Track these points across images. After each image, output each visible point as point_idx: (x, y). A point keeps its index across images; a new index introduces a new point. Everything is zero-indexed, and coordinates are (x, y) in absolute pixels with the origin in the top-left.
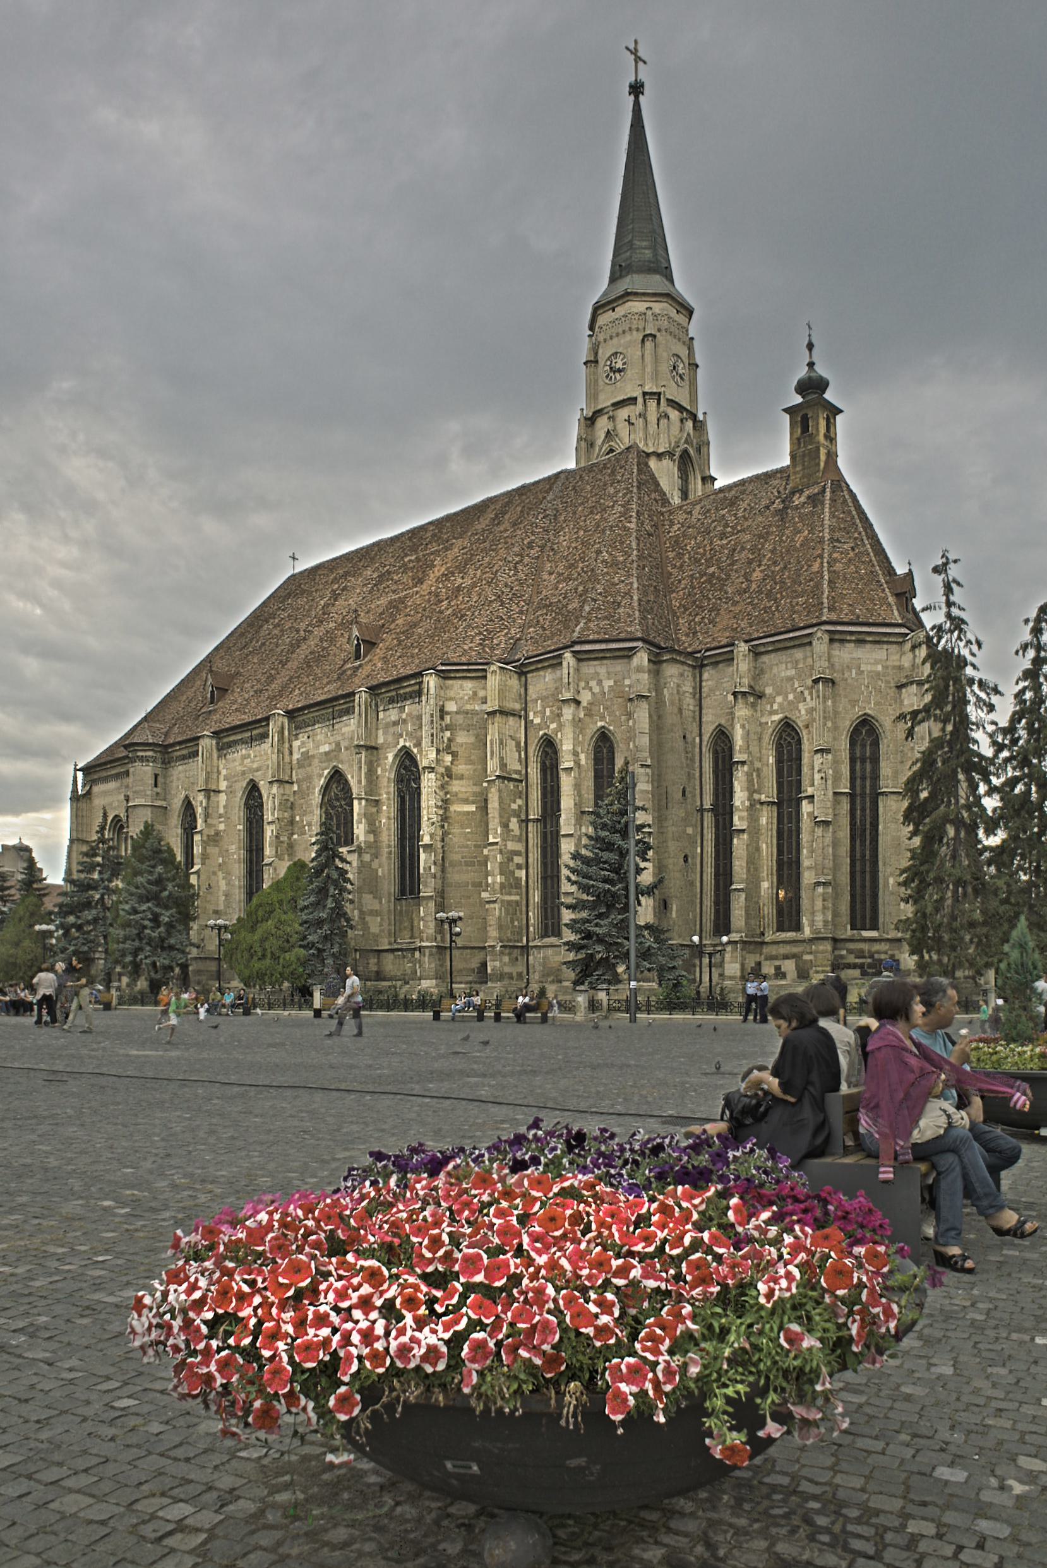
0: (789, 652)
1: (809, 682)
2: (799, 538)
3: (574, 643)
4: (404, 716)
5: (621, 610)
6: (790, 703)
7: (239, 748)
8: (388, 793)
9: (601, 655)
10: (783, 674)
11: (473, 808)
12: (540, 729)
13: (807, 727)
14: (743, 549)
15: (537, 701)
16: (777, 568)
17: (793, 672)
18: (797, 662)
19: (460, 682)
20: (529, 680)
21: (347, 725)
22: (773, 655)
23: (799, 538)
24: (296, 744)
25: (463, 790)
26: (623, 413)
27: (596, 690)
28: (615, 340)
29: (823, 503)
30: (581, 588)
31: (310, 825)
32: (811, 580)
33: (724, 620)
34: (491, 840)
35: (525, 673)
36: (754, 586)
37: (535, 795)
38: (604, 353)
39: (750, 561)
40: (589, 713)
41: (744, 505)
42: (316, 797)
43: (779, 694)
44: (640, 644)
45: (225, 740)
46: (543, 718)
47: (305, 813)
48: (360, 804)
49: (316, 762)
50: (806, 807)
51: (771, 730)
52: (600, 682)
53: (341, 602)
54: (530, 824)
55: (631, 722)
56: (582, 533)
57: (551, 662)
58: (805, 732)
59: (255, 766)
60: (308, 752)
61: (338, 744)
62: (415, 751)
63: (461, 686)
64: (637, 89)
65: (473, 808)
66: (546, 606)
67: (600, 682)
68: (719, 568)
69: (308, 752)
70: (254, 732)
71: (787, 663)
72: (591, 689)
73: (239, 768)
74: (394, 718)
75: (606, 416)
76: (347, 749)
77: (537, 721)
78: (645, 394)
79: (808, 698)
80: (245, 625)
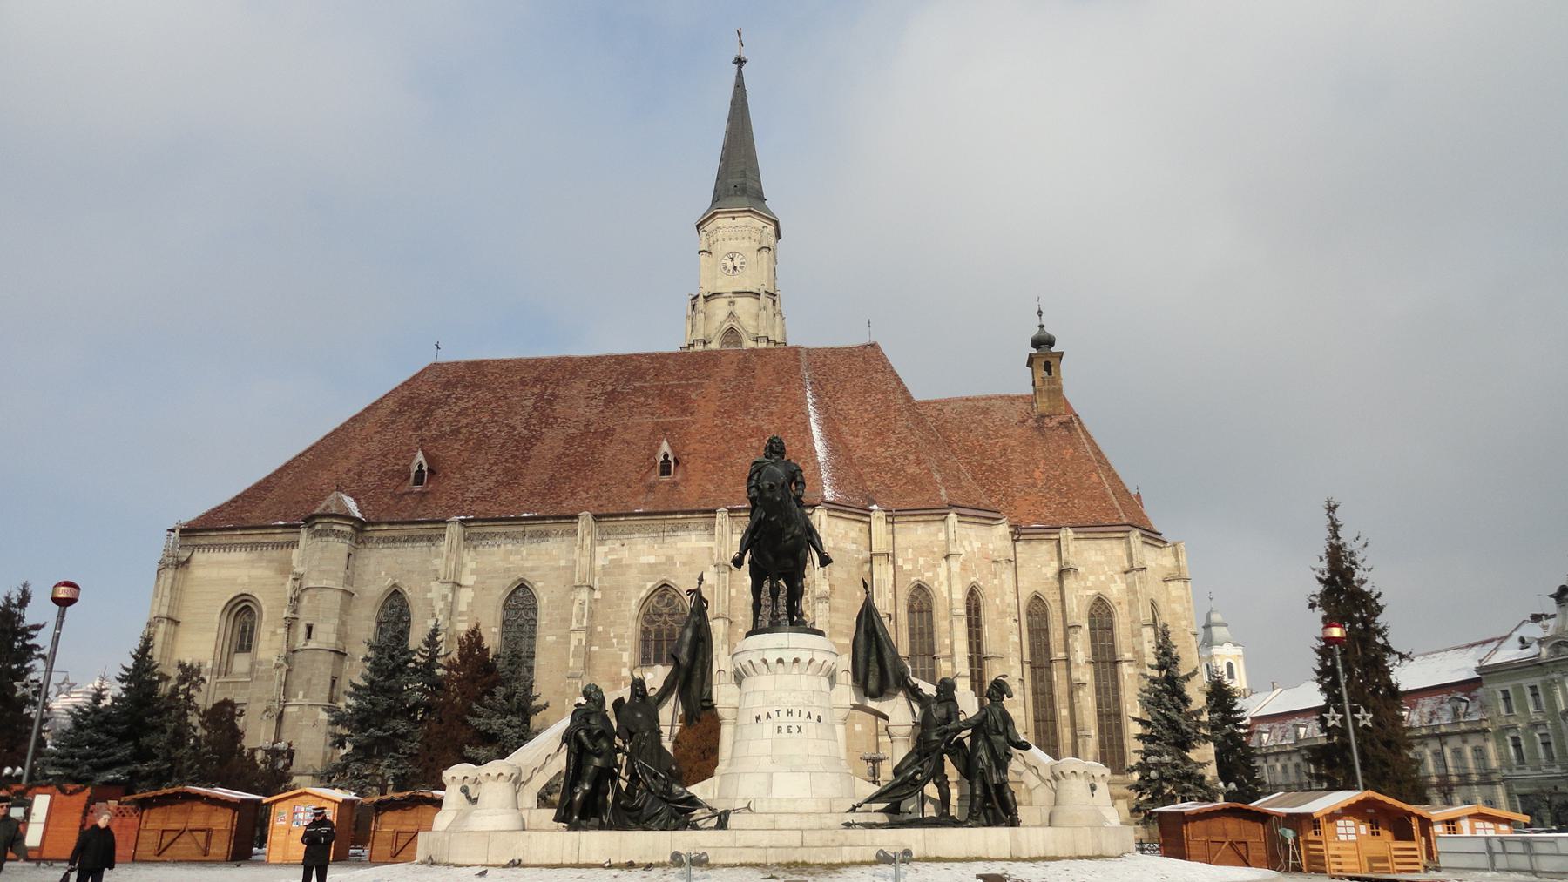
0: (1098, 541)
1: (1118, 569)
2: (1068, 453)
5: (963, 483)
6: (1102, 582)
8: (745, 616)
9: (972, 520)
10: (1093, 559)
12: (911, 575)
13: (1120, 604)
14: (1016, 451)
15: (906, 549)
16: (1057, 473)
17: (1103, 559)
18: (1105, 551)
19: (835, 520)
20: (896, 530)
21: (686, 541)
22: (1083, 542)
24: (600, 550)
25: (840, 623)
26: (742, 302)
27: (968, 549)
28: (733, 242)
29: (1076, 430)
30: (911, 457)
31: (620, 637)
32: (1095, 488)
35: (893, 523)
36: (1040, 484)
38: (721, 249)
39: (1026, 463)
40: (964, 568)
41: (997, 416)
42: (632, 607)
43: (1091, 573)
45: (476, 530)
46: (915, 567)
47: (612, 624)
48: (725, 624)
51: (1086, 602)
52: (971, 542)
53: (560, 408)
55: (996, 582)
56: (867, 406)
57: (926, 518)
59: (529, 564)
60: (622, 559)
61: (670, 559)
63: (836, 525)
64: (740, 62)
66: (870, 465)
67: (971, 542)
68: (996, 462)
69: (621, 560)
70: (529, 528)
71: (1096, 550)
72: (964, 547)
73: (500, 564)
75: (729, 299)
76: (684, 564)
77: (908, 567)
79: (1119, 581)
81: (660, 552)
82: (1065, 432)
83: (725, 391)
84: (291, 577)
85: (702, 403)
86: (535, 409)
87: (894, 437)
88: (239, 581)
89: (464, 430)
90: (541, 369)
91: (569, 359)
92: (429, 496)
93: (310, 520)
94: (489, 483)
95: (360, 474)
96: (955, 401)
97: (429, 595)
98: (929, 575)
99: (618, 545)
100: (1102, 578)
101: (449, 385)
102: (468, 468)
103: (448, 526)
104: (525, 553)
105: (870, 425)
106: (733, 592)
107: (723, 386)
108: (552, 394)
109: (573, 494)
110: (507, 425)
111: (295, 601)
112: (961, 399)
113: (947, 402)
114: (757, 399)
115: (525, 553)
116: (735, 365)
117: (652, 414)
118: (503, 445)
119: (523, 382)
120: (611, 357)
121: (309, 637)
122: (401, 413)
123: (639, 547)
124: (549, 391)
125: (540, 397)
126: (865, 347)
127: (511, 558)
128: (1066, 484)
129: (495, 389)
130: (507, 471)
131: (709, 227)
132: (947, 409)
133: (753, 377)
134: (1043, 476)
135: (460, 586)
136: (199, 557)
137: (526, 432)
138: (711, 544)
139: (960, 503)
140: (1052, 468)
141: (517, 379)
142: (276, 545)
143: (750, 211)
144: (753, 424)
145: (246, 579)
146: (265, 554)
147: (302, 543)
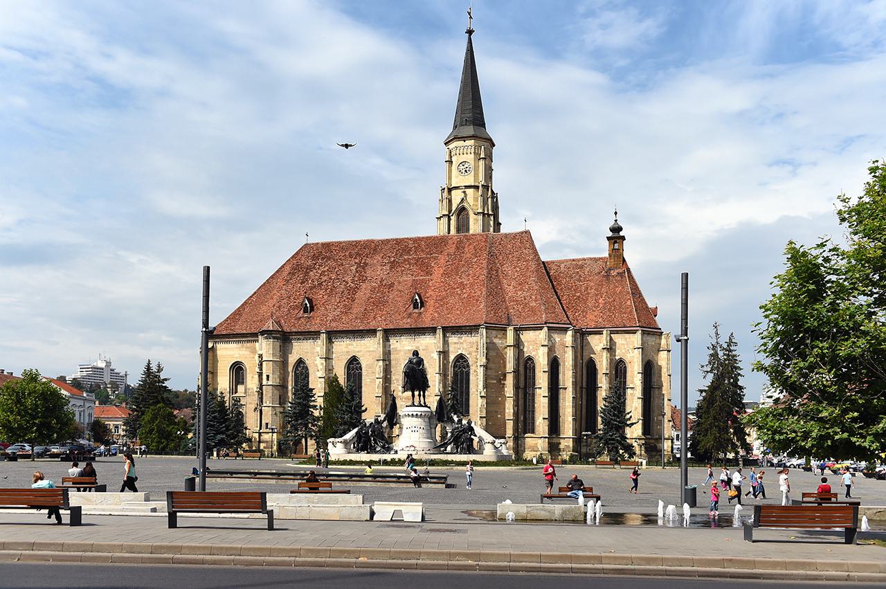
1: (632, 347)
2: (618, 290)
3: (546, 323)
4: (461, 341)
7: (345, 340)
11: (495, 382)
23: (618, 290)
26: (470, 192)
27: (553, 341)
30: (533, 297)
33: (590, 316)
34: (508, 395)
37: (522, 378)
39: (597, 295)
44: (570, 326)
49: (402, 353)
50: (629, 391)
53: (369, 272)
54: (520, 390)
58: (629, 364)
59: (357, 350)
62: (468, 356)
65: (495, 382)
66: (514, 301)
74: (455, 341)
75: (463, 190)
76: (424, 350)
78: (483, 185)
80: (288, 268)
81: (413, 345)
82: (619, 278)
83: (448, 261)
84: (257, 356)
85: (436, 269)
86: (357, 272)
87: (527, 286)
88: (235, 356)
89: (324, 283)
90: (359, 247)
91: (372, 241)
92: (311, 319)
93: (263, 333)
94: (337, 312)
95: (279, 307)
96: (567, 261)
97: (316, 362)
98: (534, 353)
99: (395, 341)
100: (623, 351)
101: (315, 257)
102: (327, 304)
103: (322, 335)
104: (355, 345)
105: (517, 279)
106: (445, 362)
107: (447, 258)
108: (364, 263)
109: (375, 318)
110: (344, 281)
111: (261, 365)
112: (570, 260)
113: (561, 262)
114: (463, 266)
115: (355, 345)
116: (455, 245)
117: (412, 275)
118: (343, 292)
119: (351, 256)
120: (393, 240)
121: (268, 379)
122: (294, 274)
123: (404, 343)
124: (363, 261)
125: (359, 264)
126: (522, 233)
127: (349, 347)
128: (614, 306)
129: (337, 259)
130: (345, 306)
131: (452, 146)
132: (562, 266)
133: (463, 253)
134: (603, 302)
135: (329, 359)
136: (219, 346)
137: (353, 285)
138: (435, 341)
139: (551, 321)
140: (609, 298)
141: (347, 254)
142: (248, 341)
143: (473, 136)
144: (459, 281)
145: (238, 355)
146: (245, 345)
147: (260, 341)
